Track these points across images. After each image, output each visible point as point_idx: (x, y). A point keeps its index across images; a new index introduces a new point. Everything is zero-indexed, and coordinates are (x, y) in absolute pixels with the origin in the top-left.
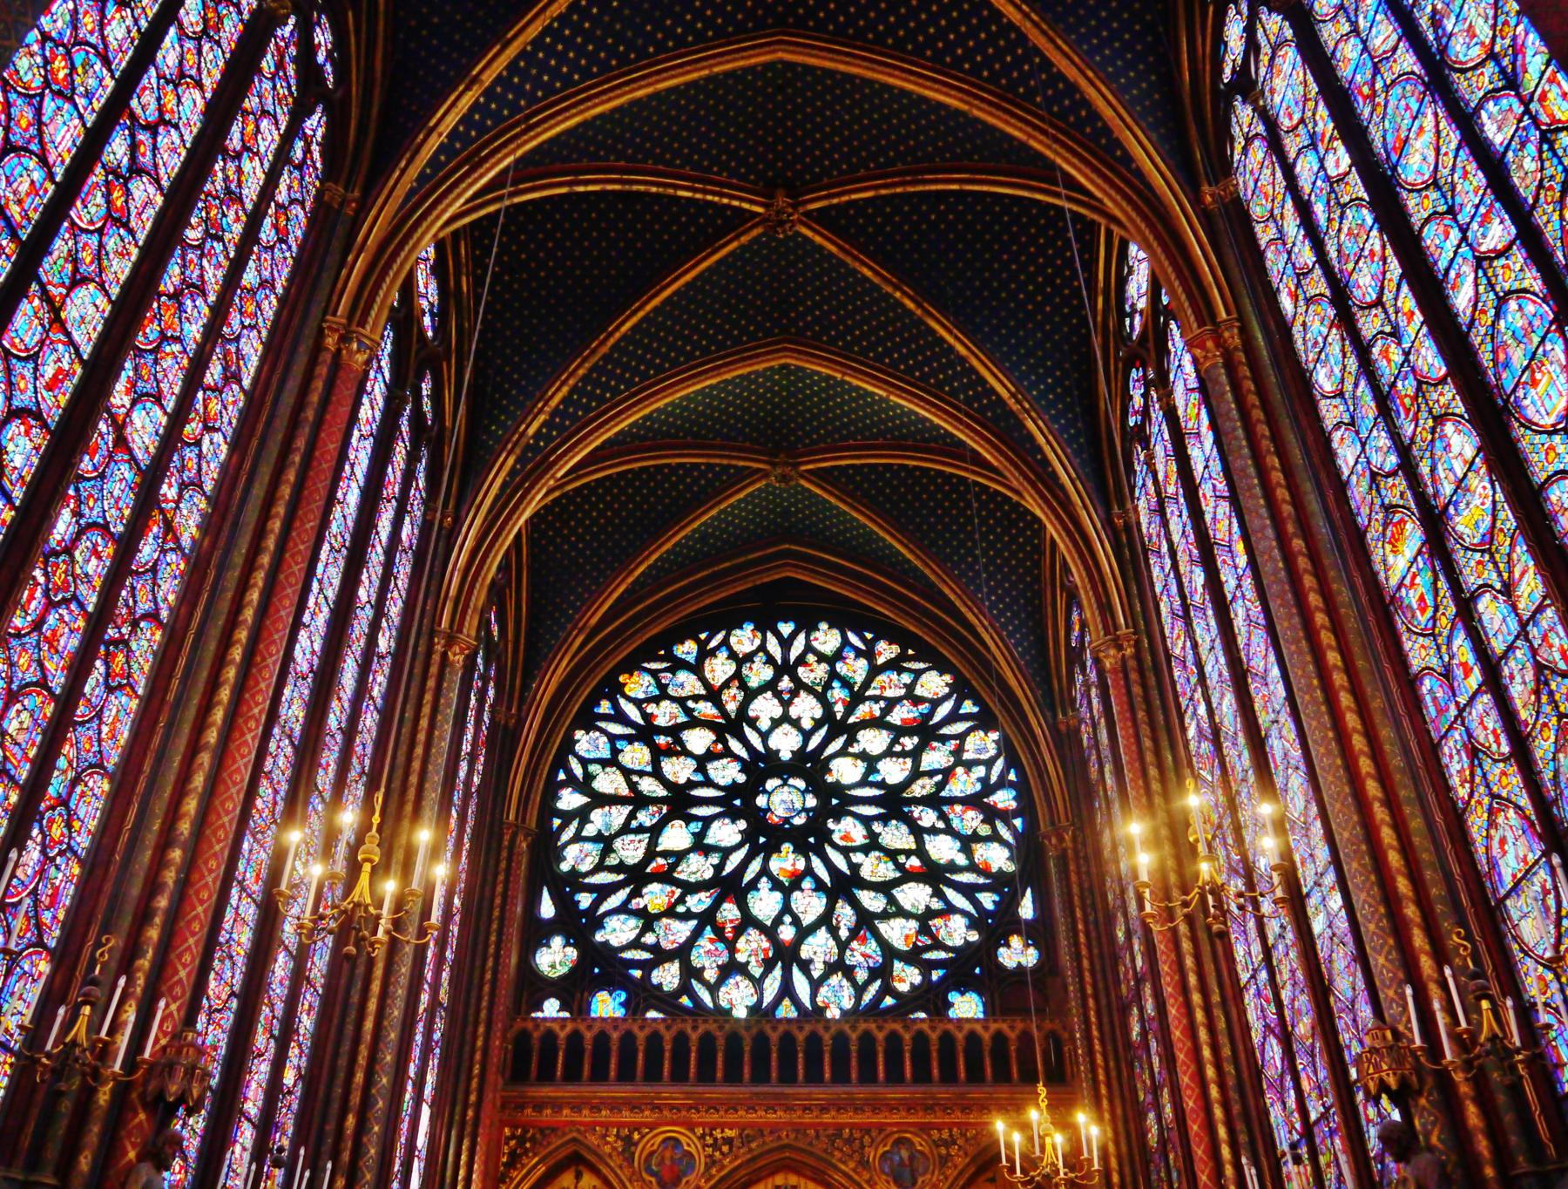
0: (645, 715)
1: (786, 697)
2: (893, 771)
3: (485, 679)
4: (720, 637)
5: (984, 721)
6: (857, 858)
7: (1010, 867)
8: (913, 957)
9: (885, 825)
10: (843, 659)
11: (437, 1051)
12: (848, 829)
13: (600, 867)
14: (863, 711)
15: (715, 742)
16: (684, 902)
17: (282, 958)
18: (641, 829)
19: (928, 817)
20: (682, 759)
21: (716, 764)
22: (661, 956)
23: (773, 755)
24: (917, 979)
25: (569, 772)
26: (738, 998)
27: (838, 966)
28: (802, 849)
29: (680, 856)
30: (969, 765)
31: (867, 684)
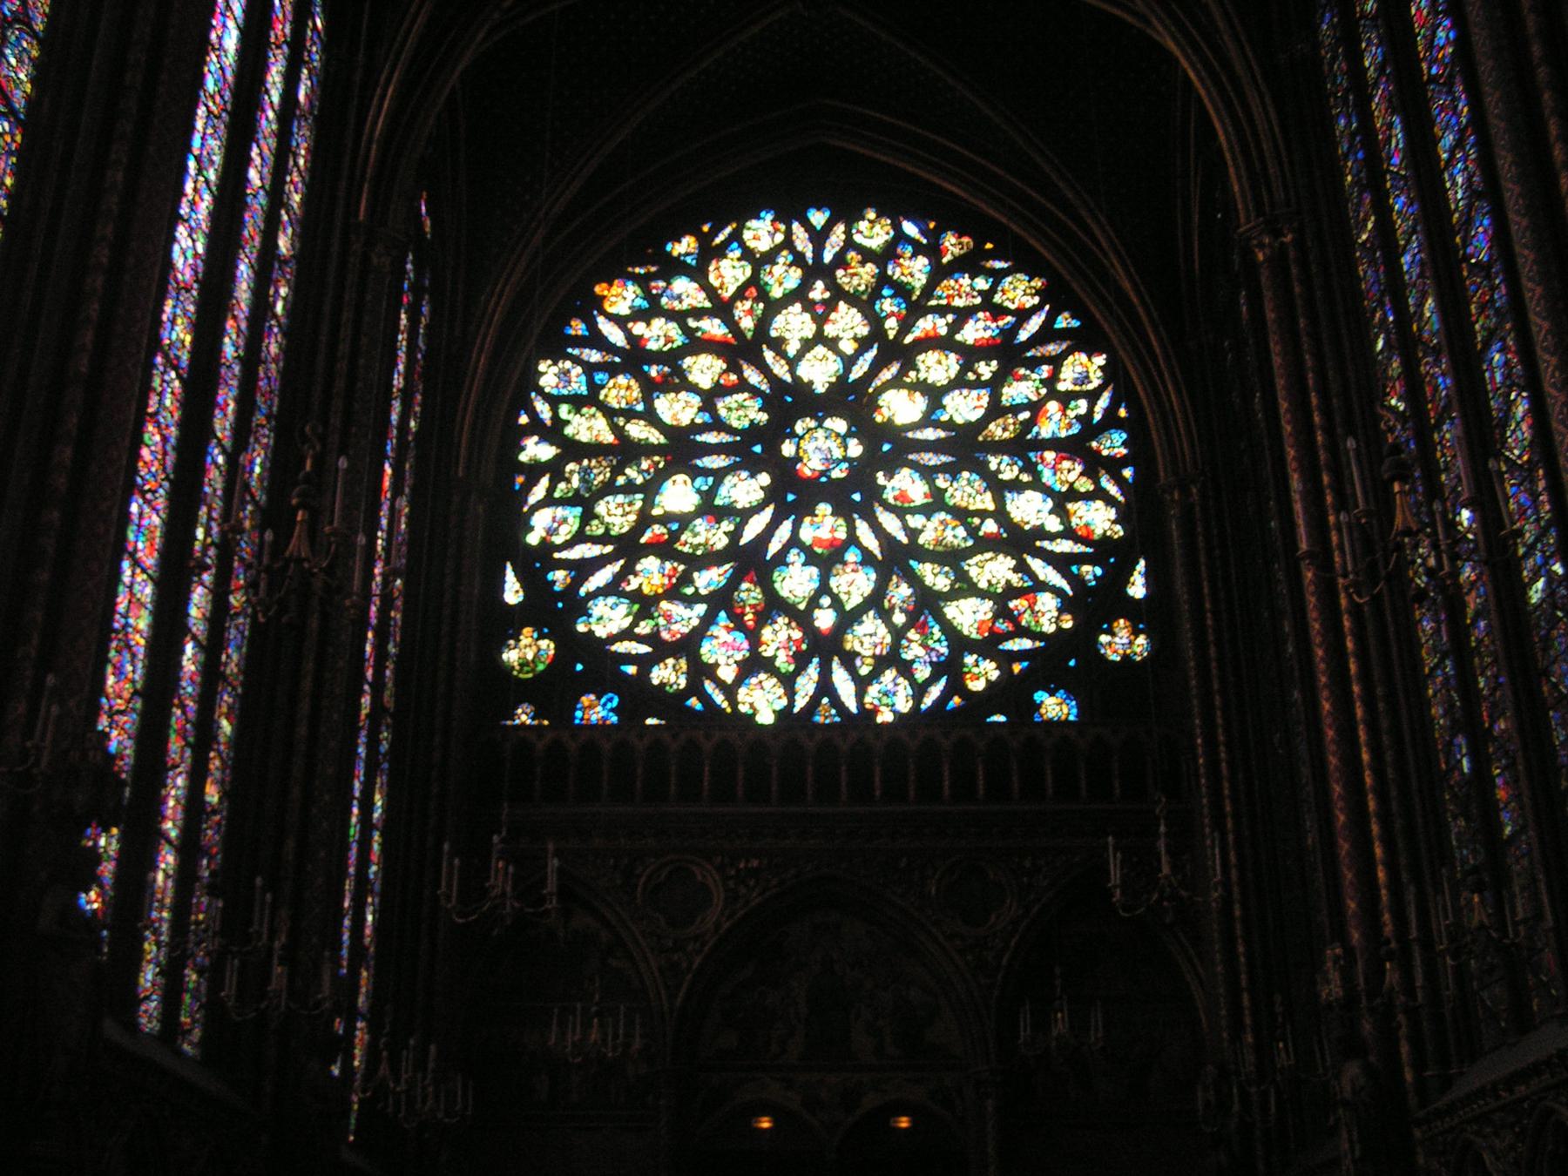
0: (629, 336)
2: (965, 407)
3: (417, 289)
4: (728, 230)
5: (1083, 341)
6: (915, 521)
7: (1119, 531)
8: (988, 646)
9: (954, 478)
11: (386, 766)
12: (906, 484)
13: (580, 537)
14: (926, 325)
15: (725, 372)
16: (691, 582)
17: (189, 648)
18: (630, 488)
19: (1008, 470)
20: (683, 395)
21: (731, 401)
22: (661, 649)
23: (801, 389)
24: (994, 675)
25: (533, 414)
26: (763, 701)
27: (891, 659)
28: (844, 510)
29: (685, 521)
31: (928, 291)
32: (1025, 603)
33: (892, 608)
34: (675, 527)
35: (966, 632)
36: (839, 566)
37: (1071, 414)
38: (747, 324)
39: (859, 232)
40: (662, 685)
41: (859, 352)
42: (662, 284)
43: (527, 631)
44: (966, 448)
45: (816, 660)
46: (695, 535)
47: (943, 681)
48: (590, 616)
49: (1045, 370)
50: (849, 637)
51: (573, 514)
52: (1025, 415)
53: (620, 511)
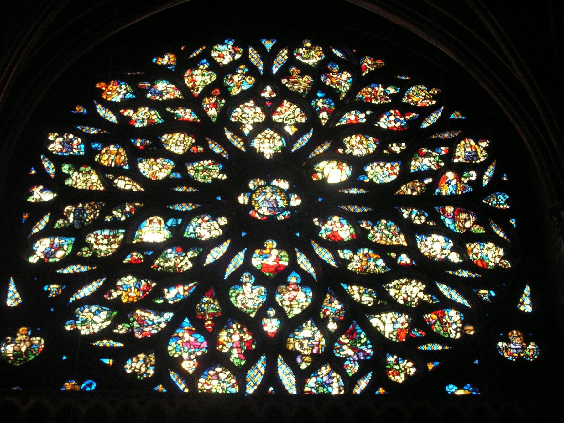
1: (269, 104)
6: (345, 254)
9: (375, 224)
10: (327, 72)
14: (350, 117)
16: (162, 295)
18: (115, 225)
23: (254, 156)
25: (42, 170)
27: (327, 357)
32: (435, 317)
33: (326, 320)
38: (213, 112)
39: (300, 55)
41: (298, 135)
42: (147, 84)
46: (166, 260)
47: (370, 375)
48: (77, 319)
49: (443, 150)
53: (106, 241)
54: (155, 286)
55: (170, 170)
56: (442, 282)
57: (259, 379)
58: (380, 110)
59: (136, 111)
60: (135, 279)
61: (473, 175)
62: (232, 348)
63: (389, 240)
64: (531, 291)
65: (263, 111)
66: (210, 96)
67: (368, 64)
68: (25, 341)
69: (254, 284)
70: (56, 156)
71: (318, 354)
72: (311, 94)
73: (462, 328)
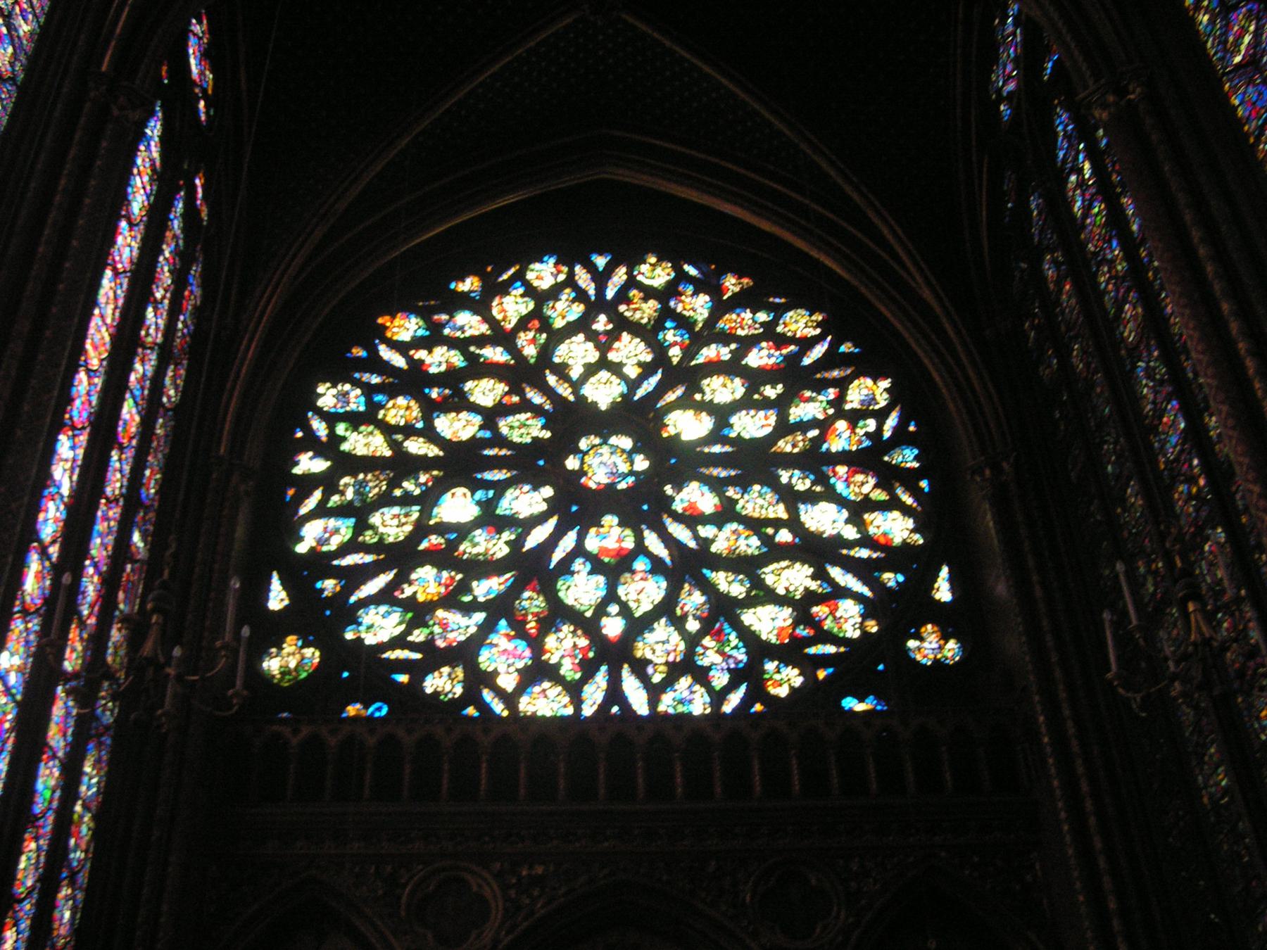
0: (410, 360)
2: (752, 426)
4: (513, 270)
6: (706, 531)
8: (790, 652)
9: (745, 490)
14: (710, 353)
15: (507, 394)
16: (469, 590)
18: (407, 500)
20: (464, 415)
22: (434, 657)
24: (798, 681)
27: (686, 666)
28: (631, 520)
29: (463, 531)
30: (854, 418)
33: (684, 617)
34: (453, 536)
35: (764, 637)
36: (627, 575)
37: (860, 432)
38: (530, 351)
40: (436, 694)
42: (444, 317)
43: (291, 639)
44: (755, 463)
45: (604, 668)
46: (475, 545)
47: (743, 688)
48: (360, 624)
49: (832, 393)
50: (640, 645)
51: (344, 529)
52: (814, 433)
53: (396, 522)
54: (461, 580)
55: (477, 428)
56: (834, 564)
57: (599, 697)
58: (748, 343)
59: (430, 352)
60: (435, 570)
61: (871, 425)
62: (563, 656)
63: (764, 511)
64: (950, 572)
65: (597, 347)
66: (526, 329)
67: (731, 284)
68: (293, 654)
69: (590, 573)
70: (328, 413)
71: (674, 663)
72: (658, 325)
73: (861, 624)
